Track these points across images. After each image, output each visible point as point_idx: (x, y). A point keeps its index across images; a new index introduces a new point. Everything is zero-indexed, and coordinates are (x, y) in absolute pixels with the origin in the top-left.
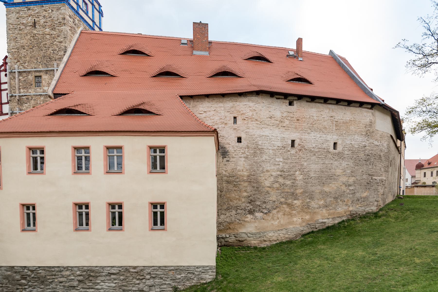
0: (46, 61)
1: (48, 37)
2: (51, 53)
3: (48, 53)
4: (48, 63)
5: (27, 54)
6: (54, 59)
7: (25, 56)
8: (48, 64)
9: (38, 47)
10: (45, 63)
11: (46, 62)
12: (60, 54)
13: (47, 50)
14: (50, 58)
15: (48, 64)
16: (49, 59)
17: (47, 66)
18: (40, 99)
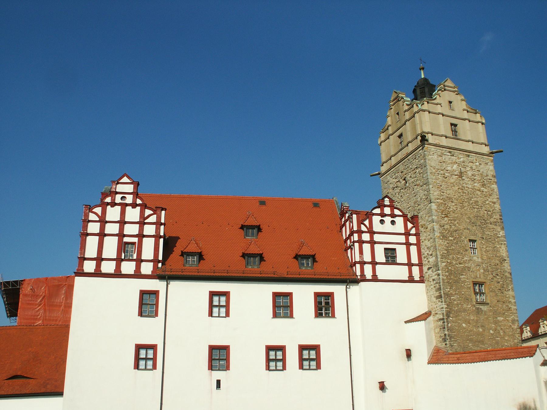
0: (481, 222)
2: (484, 213)
3: (481, 213)
4: (483, 225)
5: (456, 209)
6: (489, 221)
7: (455, 211)
8: (483, 226)
9: (469, 203)
10: (480, 225)
11: (480, 224)
12: (494, 217)
13: (480, 210)
14: (484, 220)
15: (483, 226)
16: (483, 221)
17: (482, 229)
18: (479, 271)
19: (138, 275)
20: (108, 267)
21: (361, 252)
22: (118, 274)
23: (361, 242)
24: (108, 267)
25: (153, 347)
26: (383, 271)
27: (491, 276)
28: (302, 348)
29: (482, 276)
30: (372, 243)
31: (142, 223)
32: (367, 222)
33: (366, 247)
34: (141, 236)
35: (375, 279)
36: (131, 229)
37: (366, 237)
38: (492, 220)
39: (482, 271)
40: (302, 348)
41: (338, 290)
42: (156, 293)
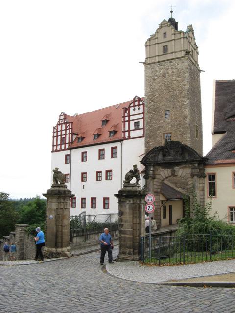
1: (175, 82)
19: (65, 149)
20: (59, 148)
21: (125, 127)
22: (61, 150)
23: (125, 122)
24: (59, 148)
25: (68, 174)
26: (134, 134)
27: (176, 128)
28: (107, 171)
29: (170, 129)
30: (129, 121)
31: (66, 130)
32: (127, 112)
33: (127, 123)
34: (66, 134)
35: (129, 138)
36: (64, 133)
37: (127, 119)
38: (182, 95)
39: (170, 126)
40: (107, 171)
41: (118, 144)
42: (69, 155)
